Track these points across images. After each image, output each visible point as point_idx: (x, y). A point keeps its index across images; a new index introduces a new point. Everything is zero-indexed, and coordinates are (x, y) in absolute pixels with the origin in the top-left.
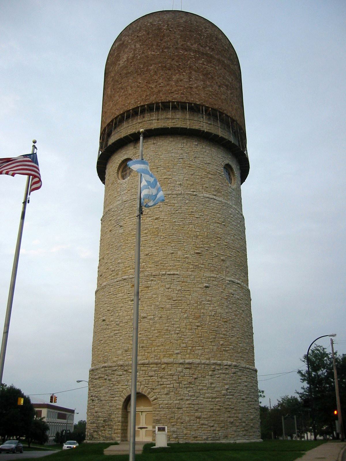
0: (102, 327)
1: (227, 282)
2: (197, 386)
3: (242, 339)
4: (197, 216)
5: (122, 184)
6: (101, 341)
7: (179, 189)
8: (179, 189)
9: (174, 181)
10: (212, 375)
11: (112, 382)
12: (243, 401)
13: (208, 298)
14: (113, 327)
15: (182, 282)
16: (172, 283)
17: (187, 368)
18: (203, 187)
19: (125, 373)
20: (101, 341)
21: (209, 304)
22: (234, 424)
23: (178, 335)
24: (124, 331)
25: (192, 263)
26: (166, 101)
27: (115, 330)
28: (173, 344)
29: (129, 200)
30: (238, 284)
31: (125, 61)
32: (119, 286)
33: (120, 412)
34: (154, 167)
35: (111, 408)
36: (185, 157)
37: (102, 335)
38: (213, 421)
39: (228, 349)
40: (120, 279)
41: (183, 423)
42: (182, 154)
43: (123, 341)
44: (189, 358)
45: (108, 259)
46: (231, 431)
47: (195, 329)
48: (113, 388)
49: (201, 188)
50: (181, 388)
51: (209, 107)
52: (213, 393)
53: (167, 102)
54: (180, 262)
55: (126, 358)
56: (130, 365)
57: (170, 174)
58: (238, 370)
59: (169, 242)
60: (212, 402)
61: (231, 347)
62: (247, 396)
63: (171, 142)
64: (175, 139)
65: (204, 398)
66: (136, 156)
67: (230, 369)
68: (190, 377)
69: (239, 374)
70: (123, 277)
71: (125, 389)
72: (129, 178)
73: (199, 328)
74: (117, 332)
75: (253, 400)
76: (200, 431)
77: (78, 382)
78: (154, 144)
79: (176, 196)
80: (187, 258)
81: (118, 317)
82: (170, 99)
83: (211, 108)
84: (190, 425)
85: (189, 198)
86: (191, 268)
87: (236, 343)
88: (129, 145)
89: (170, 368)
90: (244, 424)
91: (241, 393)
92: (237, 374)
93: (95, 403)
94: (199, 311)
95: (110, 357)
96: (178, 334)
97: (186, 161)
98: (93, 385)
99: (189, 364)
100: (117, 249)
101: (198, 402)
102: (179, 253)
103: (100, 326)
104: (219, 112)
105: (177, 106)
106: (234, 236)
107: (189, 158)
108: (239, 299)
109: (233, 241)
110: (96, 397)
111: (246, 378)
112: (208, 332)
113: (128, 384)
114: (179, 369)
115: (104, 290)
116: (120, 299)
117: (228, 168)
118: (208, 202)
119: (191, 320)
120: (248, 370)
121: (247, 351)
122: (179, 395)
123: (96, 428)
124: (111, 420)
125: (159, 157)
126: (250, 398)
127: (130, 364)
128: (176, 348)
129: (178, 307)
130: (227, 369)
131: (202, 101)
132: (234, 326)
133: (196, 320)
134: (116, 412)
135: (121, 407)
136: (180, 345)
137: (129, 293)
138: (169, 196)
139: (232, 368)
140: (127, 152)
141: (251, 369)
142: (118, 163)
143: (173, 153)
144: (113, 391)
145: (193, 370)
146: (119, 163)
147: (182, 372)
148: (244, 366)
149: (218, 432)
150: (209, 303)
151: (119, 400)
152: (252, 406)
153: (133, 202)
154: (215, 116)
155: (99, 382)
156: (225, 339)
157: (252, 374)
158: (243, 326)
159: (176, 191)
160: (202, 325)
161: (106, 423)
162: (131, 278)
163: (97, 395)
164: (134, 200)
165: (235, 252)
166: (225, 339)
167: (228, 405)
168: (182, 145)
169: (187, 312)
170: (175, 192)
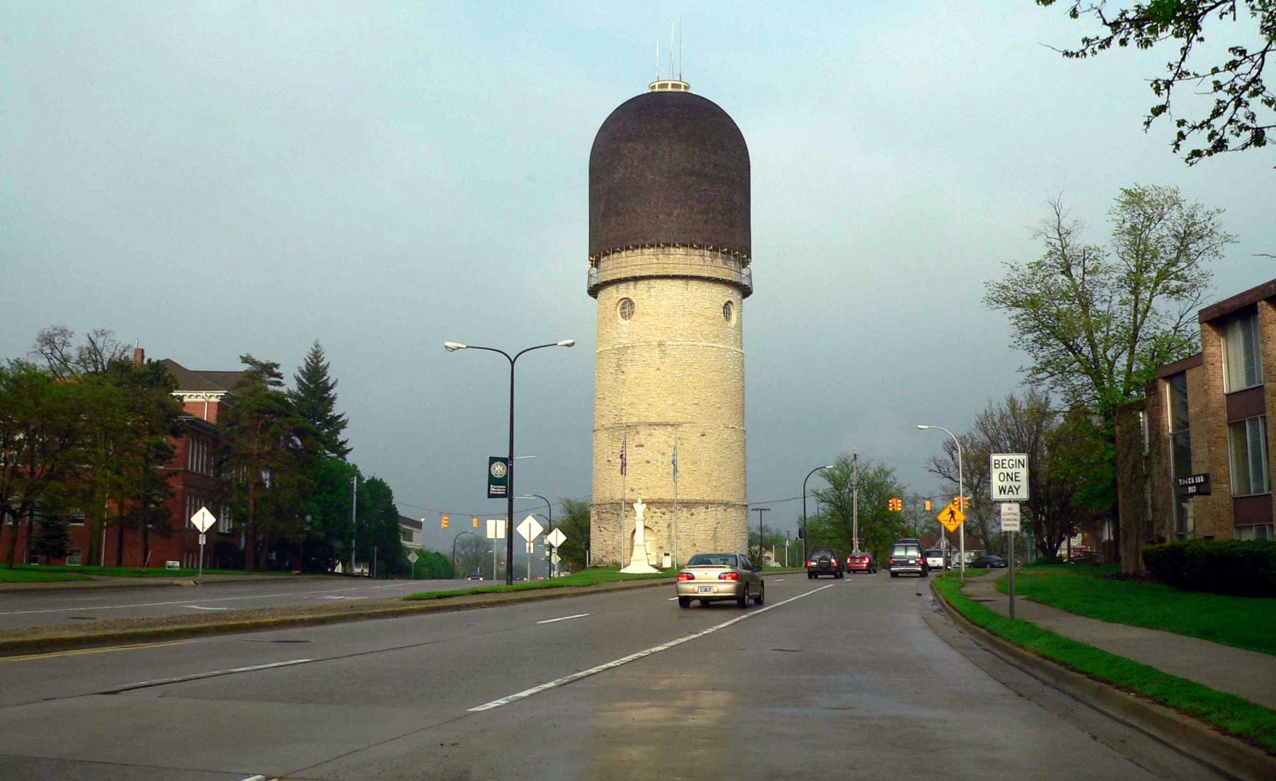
79: (676, 347)
102: (679, 404)
119: (689, 466)
135: (629, 537)
151: (628, 531)
170: (675, 343)
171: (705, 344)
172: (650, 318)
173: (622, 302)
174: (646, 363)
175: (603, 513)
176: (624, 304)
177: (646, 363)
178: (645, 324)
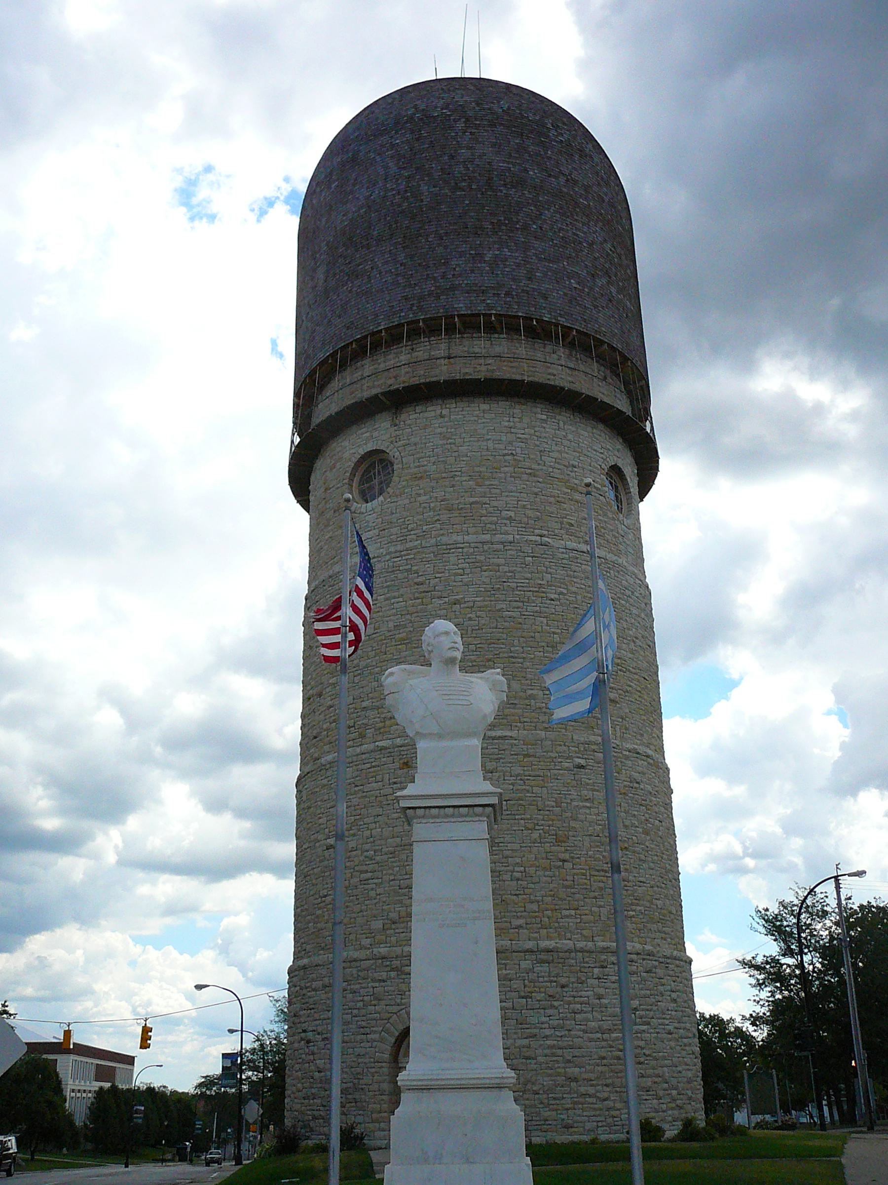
0: (326, 863)
1: (625, 753)
2: (569, 1003)
3: (661, 888)
4: (553, 596)
5: (363, 513)
6: (325, 896)
7: (504, 528)
8: (506, 528)
9: (496, 509)
10: (601, 976)
11: (361, 998)
12: (670, 1036)
13: (585, 792)
14: (356, 863)
15: (525, 756)
16: (501, 758)
17: (543, 962)
18: (562, 523)
19: (393, 974)
20: (325, 896)
21: (589, 808)
22: (654, 1093)
23: (519, 882)
24: (385, 875)
25: (544, 710)
26: (469, 312)
27: (362, 872)
28: (507, 904)
29: (384, 554)
30: (648, 756)
31: (361, 207)
32: (368, 765)
33: (385, 1070)
34: (444, 475)
35: (360, 1060)
36: (519, 450)
37: (327, 884)
38: (607, 1085)
39: (634, 913)
40: (372, 746)
41: (538, 1094)
42: (510, 443)
43: (385, 899)
44: (549, 938)
45: (333, 697)
46: (648, 1110)
47: (559, 867)
48: (363, 1012)
49: (559, 526)
50: (531, 1009)
51: (570, 329)
52: (603, 1018)
53: (472, 315)
54: (518, 706)
55: (393, 939)
56: (405, 957)
57: (485, 493)
58: (657, 963)
59: (489, 660)
60: (604, 1040)
61: (638, 908)
62: (677, 1025)
63: (484, 413)
64: (492, 405)
65: (585, 1032)
66: (396, 445)
67: (639, 961)
68: (551, 982)
69: (660, 972)
70: (377, 743)
71: (396, 1013)
72: (381, 498)
73: (568, 865)
74: (369, 875)
75: (690, 1035)
76: (578, 1112)
77: (199, 987)
78: (442, 416)
80: (532, 697)
81: (368, 841)
82: (481, 308)
83: (576, 329)
84: (555, 1099)
85: (532, 553)
86: (543, 722)
87: (649, 898)
88: (378, 417)
89: (503, 962)
90: (674, 1092)
91: (664, 1019)
92: (655, 973)
93: (315, 1049)
94: (564, 825)
95: (352, 937)
96: (518, 880)
97: (520, 461)
98: (307, 1003)
99: (549, 951)
100: (359, 674)
101: (571, 1043)
103: (321, 861)
104: (594, 338)
105: (497, 326)
106: (634, 641)
107: (527, 452)
108: (651, 793)
109: (634, 654)
110: (319, 1034)
111: (674, 982)
112: (588, 874)
113: (403, 1001)
114: (525, 964)
115: (329, 774)
116: (372, 796)
117: (616, 471)
118: (575, 561)
120: (677, 962)
121: (673, 917)
122: (527, 1026)
123: (321, 1108)
124: (362, 1089)
125: (455, 449)
126: (684, 1029)
127: (404, 954)
128: (515, 914)
129: (517, 817)
130: (632, 961)
131: (556, 314)
132: (643, 857)
133: (559, 846)
134: (373, 1070)
135: (386, 1056)
136: (525, 907)
137: (395, 783)
138: (486, 547)
139: (644, 959)
140: (375, 434)
141: (682, 960)
142: (350, 460)
143: (489, 439)
144: (364, 1018)
145: (556, 965)
146: (355, 460)
147: (532, 970)
148: (668, 953)
149: (618, 1112)
150: (588, 805)
151: (382, 1040)
152: (687, 1048)
153: (396, 560)
154: (586, 349)
155: (323, 996)
156: (627, 890)
157: (684, 971)
158: (662, 858)
159: (501, 534)
160: (573, 858)
161: (350, 1097)
162: (398, 746)
163: (320, 1029)
164: (398, 554)
165: (638, 681)
166: (627, 890)
167: (639, 1046)
168: (509, 421)
169: (537, 827)
170: (499, 537)
171: (570, 545)
172: (433, 484)
173: (363, 467)
174: (422, 588)
175: (315, 990)
176: (367, 471)
177: (422, 588)
178: (423, 498)
